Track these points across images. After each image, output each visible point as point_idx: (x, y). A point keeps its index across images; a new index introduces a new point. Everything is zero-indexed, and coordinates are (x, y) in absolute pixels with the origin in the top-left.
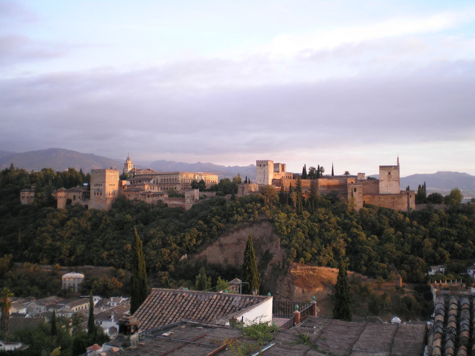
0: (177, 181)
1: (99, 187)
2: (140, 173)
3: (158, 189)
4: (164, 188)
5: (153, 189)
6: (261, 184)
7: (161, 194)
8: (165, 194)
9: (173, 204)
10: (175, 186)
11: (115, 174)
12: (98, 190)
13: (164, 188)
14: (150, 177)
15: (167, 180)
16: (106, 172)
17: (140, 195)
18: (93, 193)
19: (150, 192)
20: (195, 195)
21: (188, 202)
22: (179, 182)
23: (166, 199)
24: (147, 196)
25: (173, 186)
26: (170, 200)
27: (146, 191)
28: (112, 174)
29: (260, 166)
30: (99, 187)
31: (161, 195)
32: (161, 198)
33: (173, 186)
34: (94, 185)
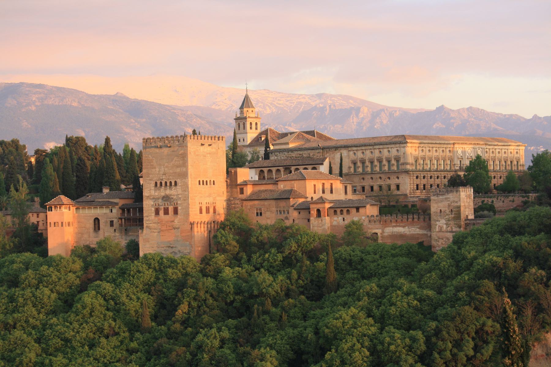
1: (168, 192)
2: (288, 143)
4: (363, 188)
5: (332, 192)
7: (356, 205)
8: (368, 206)
9: (393, 236)
10: (397, 181)
11: (214, 150)
12: (166, 198)
13: (363, 188)
14: (317, 155)
15: (372, 162)
16: (189, 145)
17: (291, 210)
18: (153, 209)
20: (462, 204)
21: (441, 228)
22: (409, 167)
23: (371, 220)
24: (314, 212)
26: (386, 224)
27: (309, 199)
28: (206, 149)
30: (168, 192)
31: (358, 209)
32: (354, 217)
33: (388, 182)
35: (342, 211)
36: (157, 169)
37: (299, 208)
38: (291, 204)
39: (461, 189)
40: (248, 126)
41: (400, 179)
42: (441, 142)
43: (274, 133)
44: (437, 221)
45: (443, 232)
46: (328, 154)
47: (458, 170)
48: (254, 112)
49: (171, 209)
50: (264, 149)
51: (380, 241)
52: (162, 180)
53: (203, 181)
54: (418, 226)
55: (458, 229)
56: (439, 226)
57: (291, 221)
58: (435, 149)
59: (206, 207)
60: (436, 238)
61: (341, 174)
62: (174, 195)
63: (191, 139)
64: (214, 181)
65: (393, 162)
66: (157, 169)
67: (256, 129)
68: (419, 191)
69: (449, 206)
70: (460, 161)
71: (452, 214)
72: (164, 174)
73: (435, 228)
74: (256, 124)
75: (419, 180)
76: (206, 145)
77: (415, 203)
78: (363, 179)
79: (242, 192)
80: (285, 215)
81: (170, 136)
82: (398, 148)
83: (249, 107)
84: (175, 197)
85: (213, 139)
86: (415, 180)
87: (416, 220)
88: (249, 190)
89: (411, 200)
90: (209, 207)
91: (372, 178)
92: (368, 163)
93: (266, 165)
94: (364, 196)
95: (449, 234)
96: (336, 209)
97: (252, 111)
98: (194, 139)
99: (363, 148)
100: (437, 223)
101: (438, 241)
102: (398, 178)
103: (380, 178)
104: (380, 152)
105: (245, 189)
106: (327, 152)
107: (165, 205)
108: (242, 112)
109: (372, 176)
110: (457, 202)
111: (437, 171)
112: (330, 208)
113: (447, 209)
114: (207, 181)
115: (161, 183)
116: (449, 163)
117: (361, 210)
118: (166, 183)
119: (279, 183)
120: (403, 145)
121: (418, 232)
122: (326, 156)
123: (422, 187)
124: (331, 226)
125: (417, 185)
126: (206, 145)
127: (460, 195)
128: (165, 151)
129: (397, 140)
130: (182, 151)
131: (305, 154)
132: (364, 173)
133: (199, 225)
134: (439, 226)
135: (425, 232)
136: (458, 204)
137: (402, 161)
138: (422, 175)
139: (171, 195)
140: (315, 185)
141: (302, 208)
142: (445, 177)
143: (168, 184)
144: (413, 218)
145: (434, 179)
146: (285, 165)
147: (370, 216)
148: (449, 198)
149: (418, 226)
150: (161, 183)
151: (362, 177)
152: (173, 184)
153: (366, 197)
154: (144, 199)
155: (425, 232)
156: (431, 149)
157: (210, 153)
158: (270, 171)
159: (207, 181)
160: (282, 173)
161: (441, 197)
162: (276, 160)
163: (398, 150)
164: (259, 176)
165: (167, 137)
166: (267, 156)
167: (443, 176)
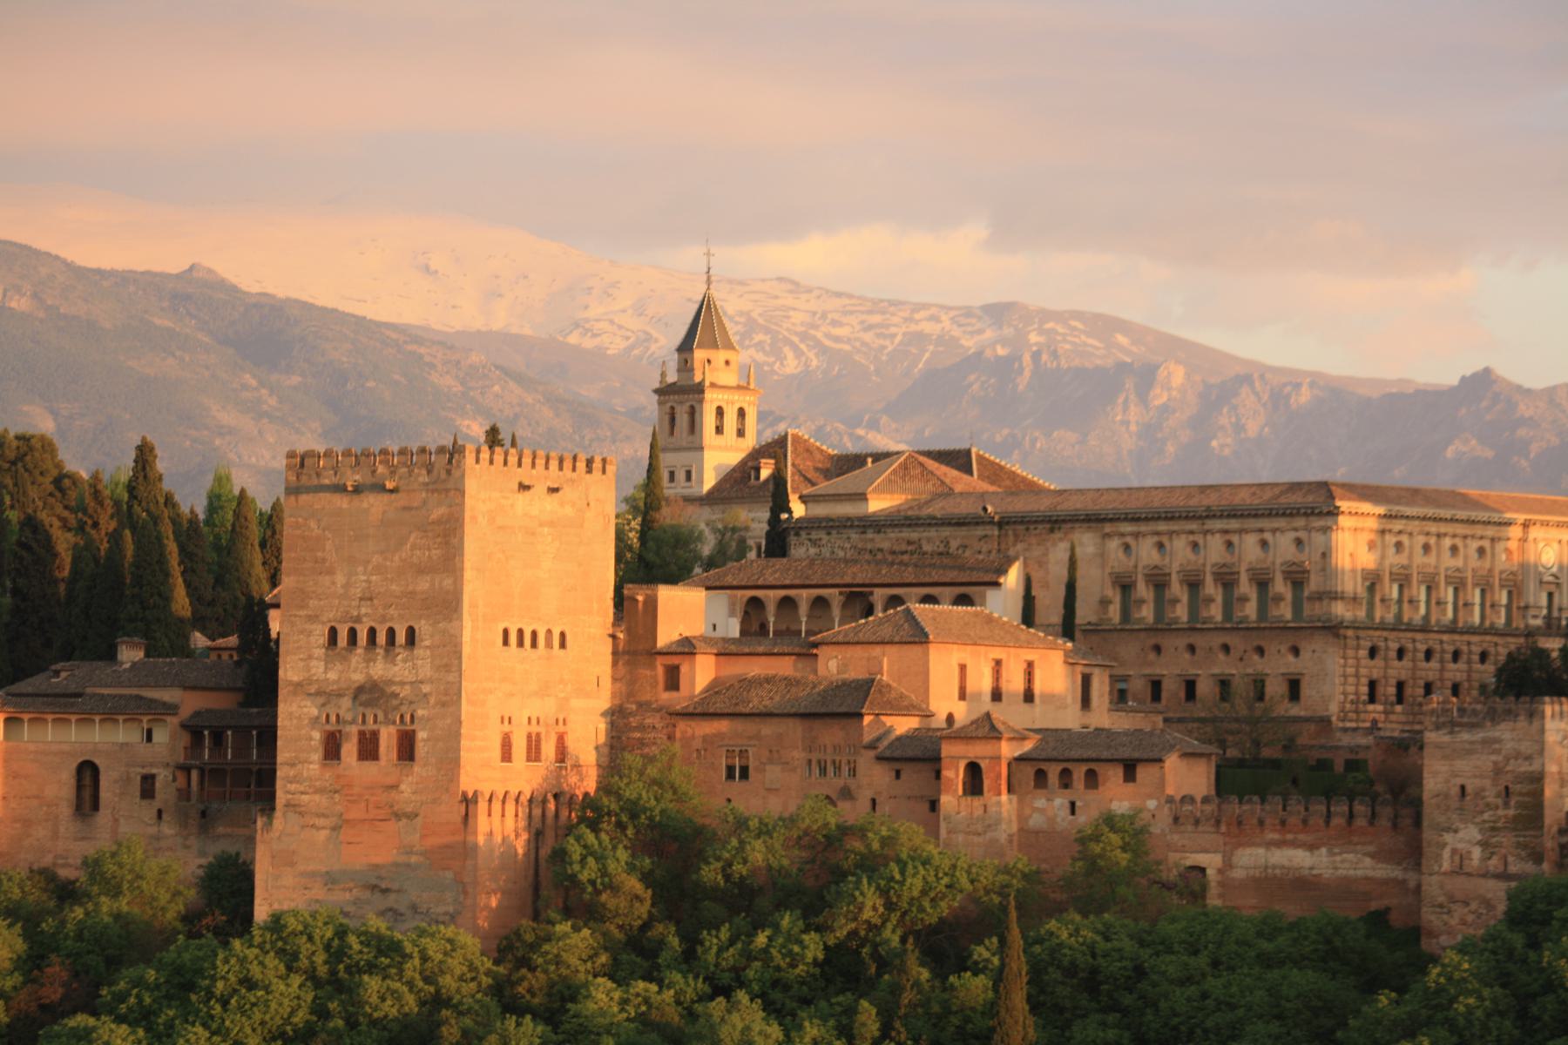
0: (1319, 597)
1: (379, 669)
3: (1086, 702)
4: (1156, 686)
7: (1126, 753)
8: (1172, 761)
9: (1268, 883)
10: (1290, 664)
11: (569, 511)
12: (370, 694)
13: (1156, 686)
14: (975, 547)
15: (1194, 585)
16: (471, 485)
17: (865, 761)
18: (317, 735)
20: (1552, 768)
21: (1461, 857)
22: (1340, 610)
23: (1181, 812)
24: (955, 775)
25: (1257, 664)
26: (1239, 833)
28: (538, 504)
30: (379, 669)
31: (1130, 770)
32: (1117, 797)
33: (1257, 664)
34: (320, 634)
35: (1066, 775)
36: (340, 579)
37: (897, 754)
38: (867, 738)
39: (1548, 710)
40: (709, 420)
41: (1306, 654)
42: (1474, 515)
43: (808, 450)
44: (1448, 830)
45: (1469, 874)
46: (1020, 546)
47: (1539, 628)
48: (733, 365)
49: (388, 739)
50: (766, 515)
51: (1214, 901)
52: (358, 619)
53: (520, 632)
54: (1371, 848)
55: (1529, 867)
56: (1454, 851)
57: (863, 804)
58: (1447, 542)
59: (529, 736)
60: (1441, 899)
61: (1068, 629)
62: (402, 683)
63: (477, 461)
64: (563, 635)
65: (1280, 586)
66: (340, 579)
67: (741, 433)
68: (1380, 708)
69: (1498, 771)
70: (1550, 595)
71: (1506, 805)
72: (368, 598)
73: (1438, 857)
74: (741, 413)
75: (1378, 662)
76: (540, 489)
77: (1361, 756)
78: (1157, 649)
80: (840, 782)
81: (395, 448)
82: (1302, 534)
83: (714, 345)
84: (405, 692)
85: (568, 464)
86: (1366, 662)
87: (1360, 822)
89: (1346, 740)
90: (538, 735)
91: (1192, 649)
92: (1177, 589)
93: (771, 580)
94: (1159, 719)
95: (1492, 884)
96: (1043, 766)
97: (727, 363)
98: (491, 462)
99: (1162, 526)
100: (1448, 837)
101: (1449, 912)
102: (1296, 651)
103: (1226, 648)
104: (1229, 544)
105: (684, 669)
106: (1016, 536)
107: (364, 722)
108: (686, 366)
109: (1191, 640)
110: (1528, 758)
111: (1452, 629)
112: (1020, 759)
113: (1487, 783)
114: (534, 634)
115: (353, 633)
116: (1504, 601)
117: (1142, 772)
118: (372, 632)
119: (822, 652)
120: (1318, 523)
121: (1371, 873)
122: (1011, 552)
123: (1392, 690)
124: (1021, 830)
125: (1372, 685)
126: (540, 489)
127: (1542, 731)
128: (374, 503)
129: (1296, 499)
130: (438, 512)
131: (930, 540)
132: (1164, 626)
133: (497, 806)
134: (1454, 851)
135: (1395, 872)
136: (1535, 767)
137: (1314, 584)
138: (1394, 646)
139: (391, 682)
140: (963, 668)
141: (910, 753)
142: (1484, 657)
143: (381, 638)
144: (1351, 816)
145: (1442, 661)
146: (848, 580)
147: (1178, 798)
148: (1498, 741)
149: (1371, 848)
150: (353, 633)
151: (1153, 641)
152: (401, 638)
153: (1166, 720)
154: (283, 692)
155: (1395, 872)
156: (1432, 541)
157: (551, 524)
159: (534, 634)
160: (836, 612)
161: (1465, 736)
162: (812, 562)
163: (1299, 542)
164: (743, 623)
165: (384, 452)
166: (778, 541)
167: (1476, 649)
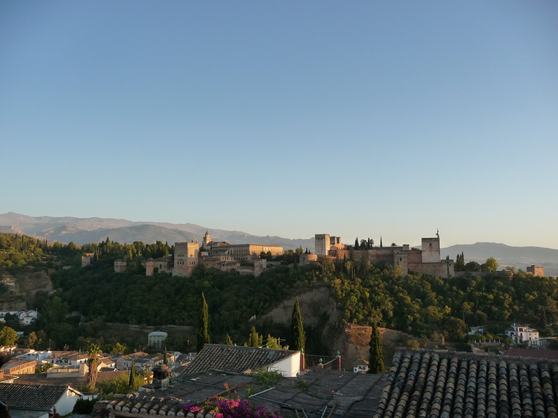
1: (181, 258)
4: (237, 258)
5: (228, 259)
6: (319, 255)
8: (237, 264)
9: (243, 272)
11: (195, 247)
12: (181, 260)
13: (237, 258)
16: (188, 245)
17: (216, 264)
18: (177, 263)
19: (224, 261)
25: (244, 257)
26: (242, 269)
29: (319, 239)
30: (181, 258)
32: (234, 267)
34: (177, 256)
79: (203, 258)
88: (204, 258)
108: (205, 236)
158: (211, 253)
